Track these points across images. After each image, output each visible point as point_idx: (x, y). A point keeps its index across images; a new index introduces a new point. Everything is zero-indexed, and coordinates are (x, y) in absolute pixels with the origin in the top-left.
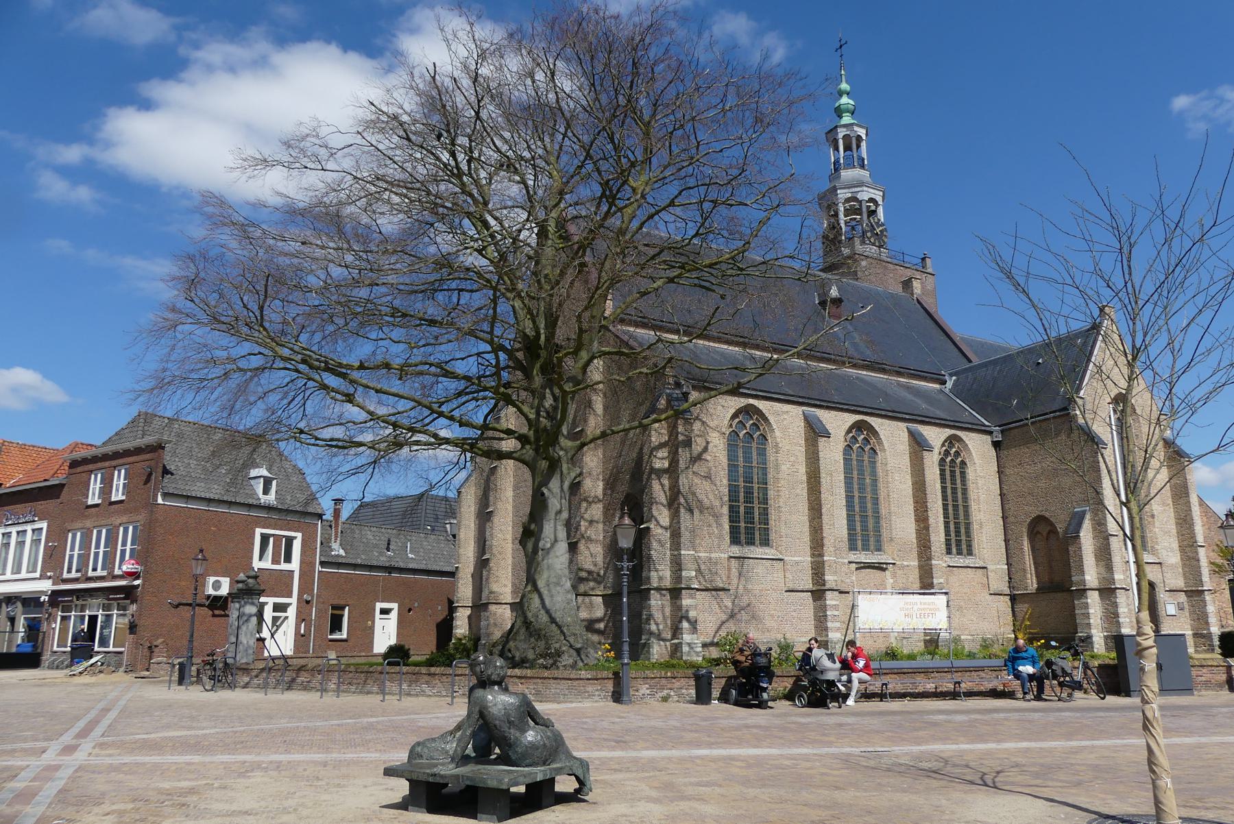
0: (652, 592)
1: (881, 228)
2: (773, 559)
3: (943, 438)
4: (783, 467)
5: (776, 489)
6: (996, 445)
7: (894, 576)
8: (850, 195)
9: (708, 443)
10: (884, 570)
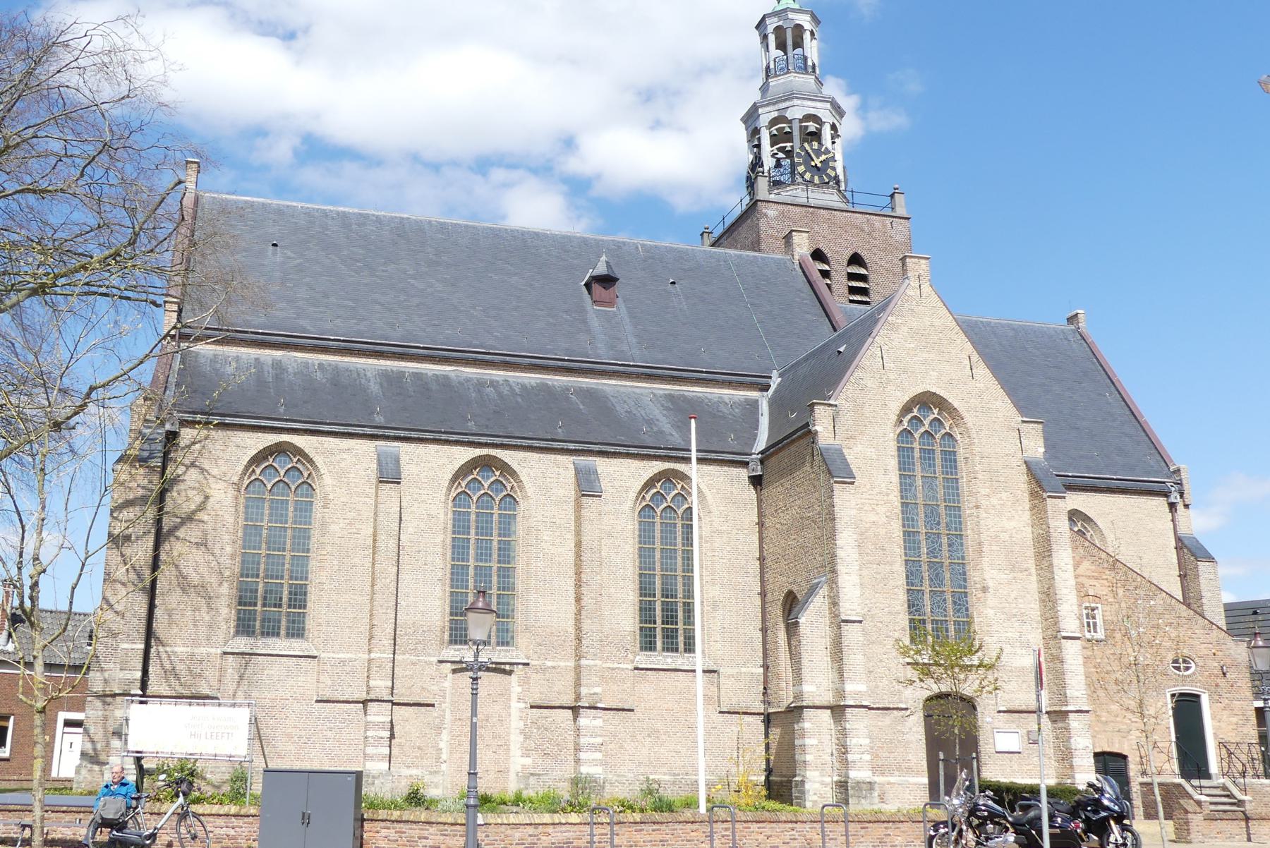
0: (89, 699)
1: (823, 157)
4: (333, 528)
5: (319, 557)
6: (756, 481)
7: (525, 682)
8: (775, 114)
9: (207, 498)
10: (510, 673)
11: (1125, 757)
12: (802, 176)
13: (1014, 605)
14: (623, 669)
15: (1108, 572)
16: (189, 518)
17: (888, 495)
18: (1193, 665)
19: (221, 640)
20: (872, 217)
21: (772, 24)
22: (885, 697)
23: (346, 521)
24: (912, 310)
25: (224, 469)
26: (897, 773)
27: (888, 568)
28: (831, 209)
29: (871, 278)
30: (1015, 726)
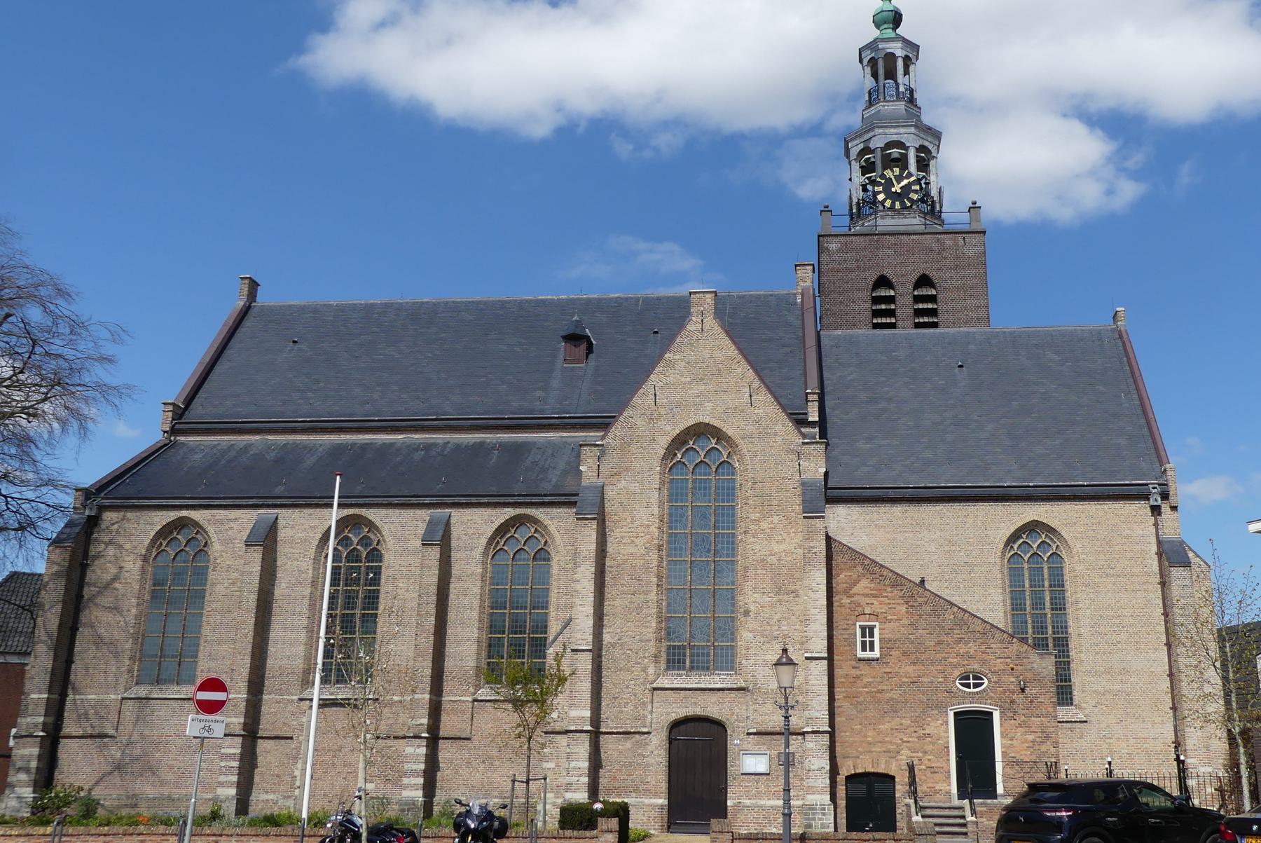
2: (184, 699)
3: (422, 526)
8: (861, 146)
9: (121, 568)
11: (893, 778)
12: (883, 203)
13: (777, 628)
14: (464, 701)
15: (889, 589)
16: (107, 586)
17: (648, 526)
18: (986, 681)
19: (122, 688)
20: (942, 236)
21: (868, 56)
22: (628, 722)
23: (230, 581)
24: (692, 345)
25: (135, 543)
26: (634, 795)
27: (642, 597)
28: (898, 234)
29: (939, 299)
30: (765, 748)
